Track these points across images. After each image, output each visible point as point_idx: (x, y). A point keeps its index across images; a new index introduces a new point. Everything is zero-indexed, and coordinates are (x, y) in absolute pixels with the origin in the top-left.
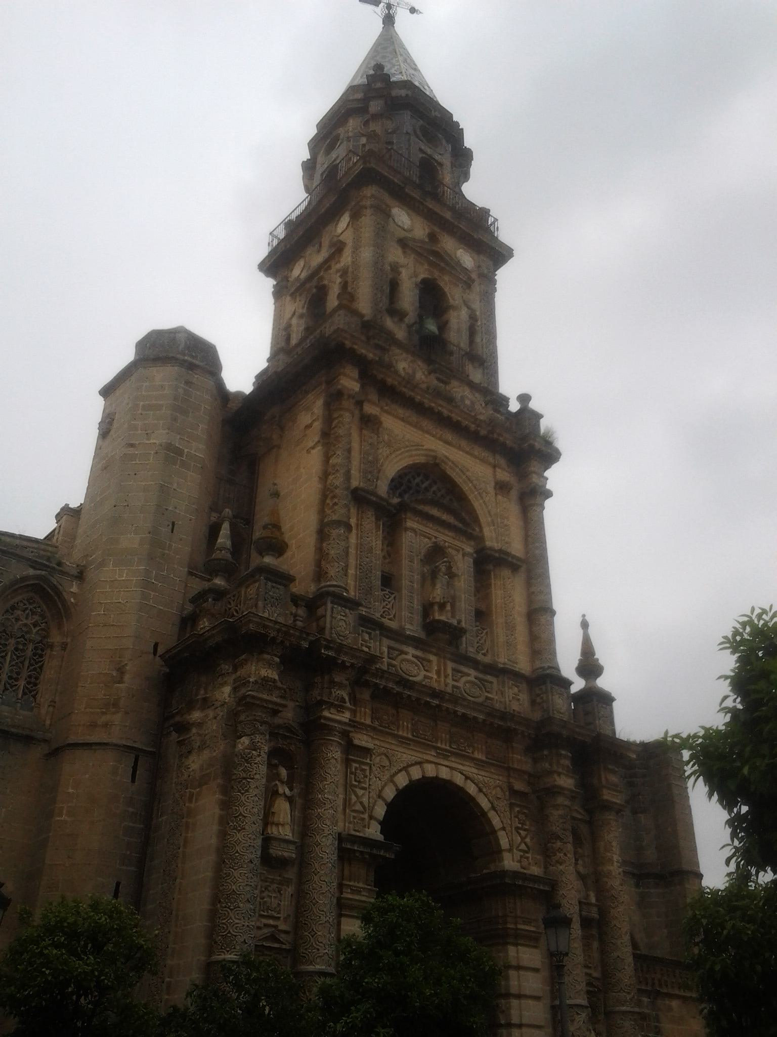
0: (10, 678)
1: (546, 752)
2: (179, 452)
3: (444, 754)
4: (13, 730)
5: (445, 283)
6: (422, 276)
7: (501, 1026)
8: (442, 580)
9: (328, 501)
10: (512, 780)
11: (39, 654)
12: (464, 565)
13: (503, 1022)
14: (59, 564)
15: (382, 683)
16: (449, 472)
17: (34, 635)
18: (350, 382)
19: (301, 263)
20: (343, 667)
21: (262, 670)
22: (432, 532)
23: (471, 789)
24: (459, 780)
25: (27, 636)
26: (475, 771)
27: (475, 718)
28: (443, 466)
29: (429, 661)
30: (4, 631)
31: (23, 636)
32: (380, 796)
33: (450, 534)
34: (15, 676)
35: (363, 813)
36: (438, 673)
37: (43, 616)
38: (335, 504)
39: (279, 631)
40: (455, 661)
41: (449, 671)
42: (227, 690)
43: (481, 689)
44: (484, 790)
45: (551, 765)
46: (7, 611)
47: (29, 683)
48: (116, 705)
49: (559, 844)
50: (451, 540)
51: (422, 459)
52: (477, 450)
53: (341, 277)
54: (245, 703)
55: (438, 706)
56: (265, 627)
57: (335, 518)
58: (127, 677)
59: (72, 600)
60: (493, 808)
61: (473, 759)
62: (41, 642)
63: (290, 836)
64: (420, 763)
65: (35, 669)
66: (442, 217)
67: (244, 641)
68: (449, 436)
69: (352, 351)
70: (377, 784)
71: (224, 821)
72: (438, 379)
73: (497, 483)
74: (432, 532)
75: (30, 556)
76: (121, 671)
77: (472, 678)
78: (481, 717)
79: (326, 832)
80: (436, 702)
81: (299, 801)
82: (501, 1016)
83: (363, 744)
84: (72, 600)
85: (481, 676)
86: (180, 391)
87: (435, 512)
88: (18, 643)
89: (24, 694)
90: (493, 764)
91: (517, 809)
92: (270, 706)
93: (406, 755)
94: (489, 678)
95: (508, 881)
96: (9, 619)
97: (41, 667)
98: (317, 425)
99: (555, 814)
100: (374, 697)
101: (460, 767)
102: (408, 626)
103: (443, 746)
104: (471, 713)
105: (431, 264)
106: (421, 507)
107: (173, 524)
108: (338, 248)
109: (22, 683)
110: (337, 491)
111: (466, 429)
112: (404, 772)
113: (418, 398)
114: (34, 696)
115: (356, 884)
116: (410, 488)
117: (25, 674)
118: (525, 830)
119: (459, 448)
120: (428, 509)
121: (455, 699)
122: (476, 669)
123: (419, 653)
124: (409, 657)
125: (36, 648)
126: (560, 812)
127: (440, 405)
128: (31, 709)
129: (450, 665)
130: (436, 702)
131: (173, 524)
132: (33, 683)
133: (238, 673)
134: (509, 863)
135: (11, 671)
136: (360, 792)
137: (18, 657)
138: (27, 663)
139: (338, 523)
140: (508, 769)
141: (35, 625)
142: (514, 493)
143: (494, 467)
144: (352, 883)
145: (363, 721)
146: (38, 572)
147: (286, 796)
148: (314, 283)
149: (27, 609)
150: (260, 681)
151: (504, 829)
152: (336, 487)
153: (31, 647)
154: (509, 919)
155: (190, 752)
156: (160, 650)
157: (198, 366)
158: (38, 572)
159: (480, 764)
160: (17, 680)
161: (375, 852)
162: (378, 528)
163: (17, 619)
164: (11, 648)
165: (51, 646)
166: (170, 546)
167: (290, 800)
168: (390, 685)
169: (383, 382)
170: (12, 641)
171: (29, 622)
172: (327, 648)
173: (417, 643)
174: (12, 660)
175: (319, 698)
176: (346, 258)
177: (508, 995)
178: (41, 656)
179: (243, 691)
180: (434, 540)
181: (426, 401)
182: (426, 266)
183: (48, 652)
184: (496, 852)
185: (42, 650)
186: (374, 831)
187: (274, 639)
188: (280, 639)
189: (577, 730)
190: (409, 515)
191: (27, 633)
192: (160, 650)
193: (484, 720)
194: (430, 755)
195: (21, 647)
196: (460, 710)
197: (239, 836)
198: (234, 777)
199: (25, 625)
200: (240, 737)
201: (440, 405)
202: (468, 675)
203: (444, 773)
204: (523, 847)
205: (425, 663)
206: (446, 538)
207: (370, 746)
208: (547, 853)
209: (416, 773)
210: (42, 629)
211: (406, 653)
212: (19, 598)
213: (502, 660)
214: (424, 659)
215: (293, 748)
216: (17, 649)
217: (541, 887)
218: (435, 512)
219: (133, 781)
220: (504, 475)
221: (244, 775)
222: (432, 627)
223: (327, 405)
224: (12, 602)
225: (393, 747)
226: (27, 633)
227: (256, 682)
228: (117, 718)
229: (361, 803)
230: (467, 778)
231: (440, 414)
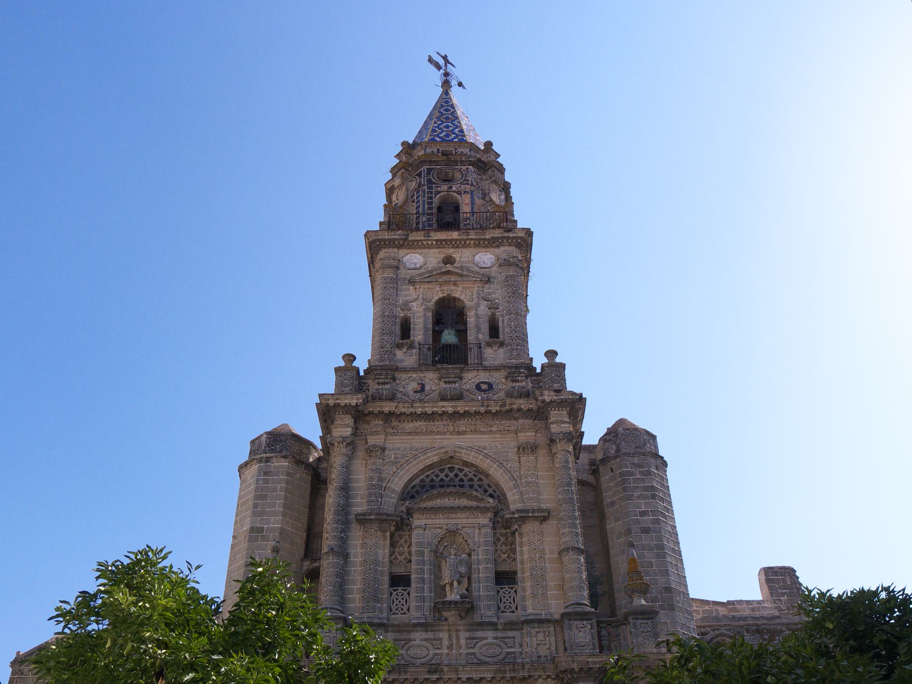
2: (260, 530)
22: (442, 521)
29: (440, 639)
33: (463, 516)
40: (469, 630)
41: (463, 642)
43: (499, 646)
50: (465, 521)
66: (451, 241)
69: (337, 406)
72: (445, 382)
74: (442, 521)
77: (490, 640)
80: (435, 677)
85: (500, 634)
86: (261, 482)
94: (510, 634)
119: (476, 432)
122: (497, 630)
123: (424, 635)
124: (417, 642)
127: (443, 407)
162: (385, 539)
169: (381, 413)
180: (445, 527)
181: (427, 409)
189: (590, 660)
190: (415, 516)
201: (443, 407)
206: (458, 521)
214: (435, 639)
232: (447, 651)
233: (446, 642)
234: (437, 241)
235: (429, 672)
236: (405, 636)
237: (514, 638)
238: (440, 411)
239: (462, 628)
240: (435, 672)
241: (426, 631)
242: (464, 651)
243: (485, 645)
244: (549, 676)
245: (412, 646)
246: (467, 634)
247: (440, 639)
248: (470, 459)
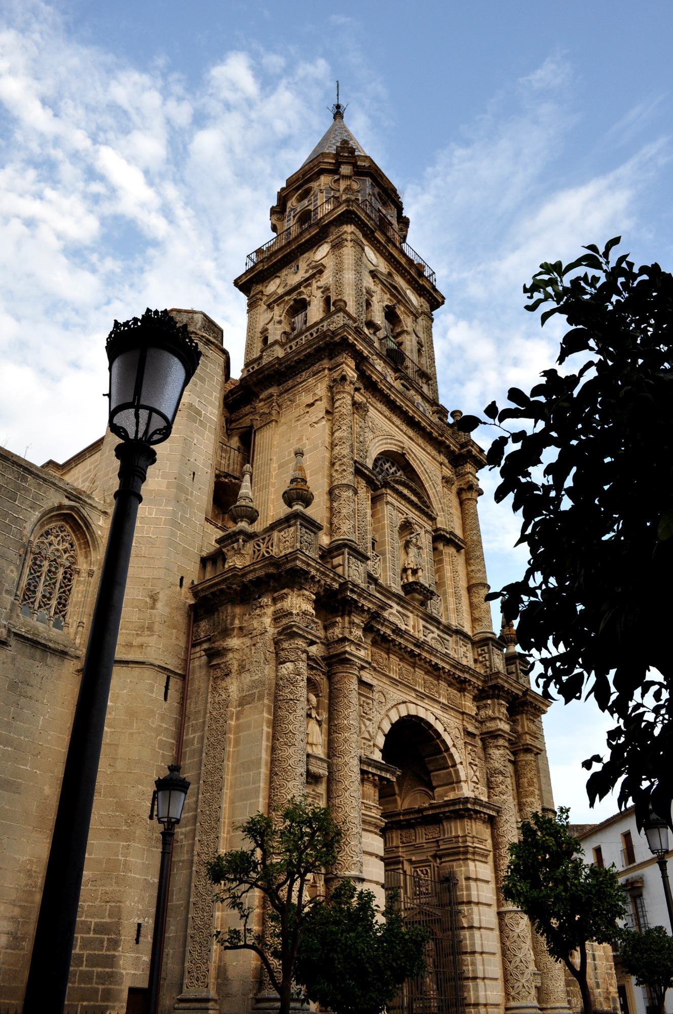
0: (44, 596)
1: (489, 702)
2: (199, 413)
3: (422, 696)
4: (50, 645)
5: (400, 310)
6: (386, 303)
7: (464, 928)
8: (413, 551)
9: (337, 467)
10: (465, 723)
11: (68, 578)
12: (425, 540)
13: (466, 925)
14: (89, 497)
15: (383, 630)
16: (412, 462)
17: (64, 560)
18: (349, 370)
19: (277, 281)
20: (362, 610)
21: (299, 603)
23: (439, 728)
24: (431, 720)
25: (59, 560)
26: (441, 713)
27: (443, 668)
28: (407, 456)
29: (408, 617)
30: (40, 553)
31: (55, 560)
32: (379, 728)
34: (48, 595)
35: (370, 741)
36: (414, 627)
37: (72, 545)
38: (344, 470)
42: (267, 621)
45: (493, 712)
46: (42, 536)
47: (59, 603)
48: (150, 628)
49: (501, 778)
51: (394, 448)
52: (429, 448)
53: (323, 292)
54: (288, 633)
55: (419, 655)
56: (308, 565)
57: (344, 482)
58: (159, 605)
59: (99, 533)
60: (454, 746)
62: (69, 567)
63: (322, 756)
64: (404, 702)
65: (64, 592)
67: (283, 576)
68: (411, 433)
69: (353, 346)
70: (377, 717)
71: (274, 737)
72: (403, 385)
73: (443, 478)
75: (67, 488)
76: (154, 599)
78: (447, 667)
79: (353, 754)
81: (325, 726)
82: (464, 920)
83: (369, 681)
84: (99, 533)
85: (441, 634)
87: (406, 491)
88: (50, 565)
89: (56, 613)
90: (452, 709)
91: (470, 747)
92: (310, 637)
93: (396, 694)
95: (469, 806)
96: (43, 543)
97: (69, 590)
98: (323, 405)
99: (496, 753)
102: (393, 585)
104: (441, 664)
105: (392, 295)
106: (397, 486)
107: (194, 474)
108: (319, 270)
109: (54, 602)
110: (345, 460)
111: (424, 429)
112: (395, 709)
113: (393, 397)
114: (64, 616)
116: (382, 471)
117: (56, 595)
120: (401, 488)
122: (438, 628)
124: (394, 611)
125: (65, 573)
126: (501, 752)
128: (61, 628)
129: (422, 622)
130: (417, 651)
131: (194, 474)
132: (63, 604)
133: (279, 606)
134: (467, 791)
135: (45, 590)
136: (368, 723)
137: (51, 579)
138: (58, 585)
139: (348, 486)
140: (463, 713)
141: (65, 552)
142: (454, 489)
143: (441, 464)
146: (72, 503)
147: (317, 720)
148: (294, 296)
149: (58, 535)
151: (461, 763)
152: (344, 457)
153: (61, 570)
154: (468, 839)
155: (227, 675)
156: (187, 583)
157: (212, 343)
158: (72, 503)
159: (445, 707)
160: (49, 599)
161: (383, 774)
163: (50, 544)
164: (45, 569)
165: (78, 573)
166: (192, 493)
167: (319, 723)
168: (389, 632)
170: (46, 563)
171: (60, 547)
172: (352, 591)
173: (400, 600)
174: (46, 580)
175: (340, 636)
176: (327, 278)
177: (469, 903)
178: (70, 580)
179: (285, 621)
182: (388, 296)
183: (75, 577)
184: (454, 782)
185: (71, 575)
186: (377, 756)
187: (313, 577)
191: (59, 557)
192: (187, 583)
194: (411, 697)
195: (53, 569)
196: (435, 660)
197: (291, 750)
198: (281, 698)
199: (58, 550)
200: (284, 662)
202: (433, 632)
203: (422, 714)
204: (475, 779)
207: (374, 682)
208: (490, 786)
210: (72, 556)
211: (391, 607)
212: (53, 525)
213: (454, 623)
214: (404, 615)
215: (318, 678)
216: (49, 571)
218: (406, 491)
219: (166, 699)
220: (448, 472)
221: (292, 697)
222: (409, 588)
223: (330, 388)
224: (46, 528)
226: (59, 557)
227: (298, 614)
228: (152, 641)
229: (368, 732)
230: (437, 718)
231: (406, 413)
234: (390, 254)
238: (405, 408)
248: (415, 466)
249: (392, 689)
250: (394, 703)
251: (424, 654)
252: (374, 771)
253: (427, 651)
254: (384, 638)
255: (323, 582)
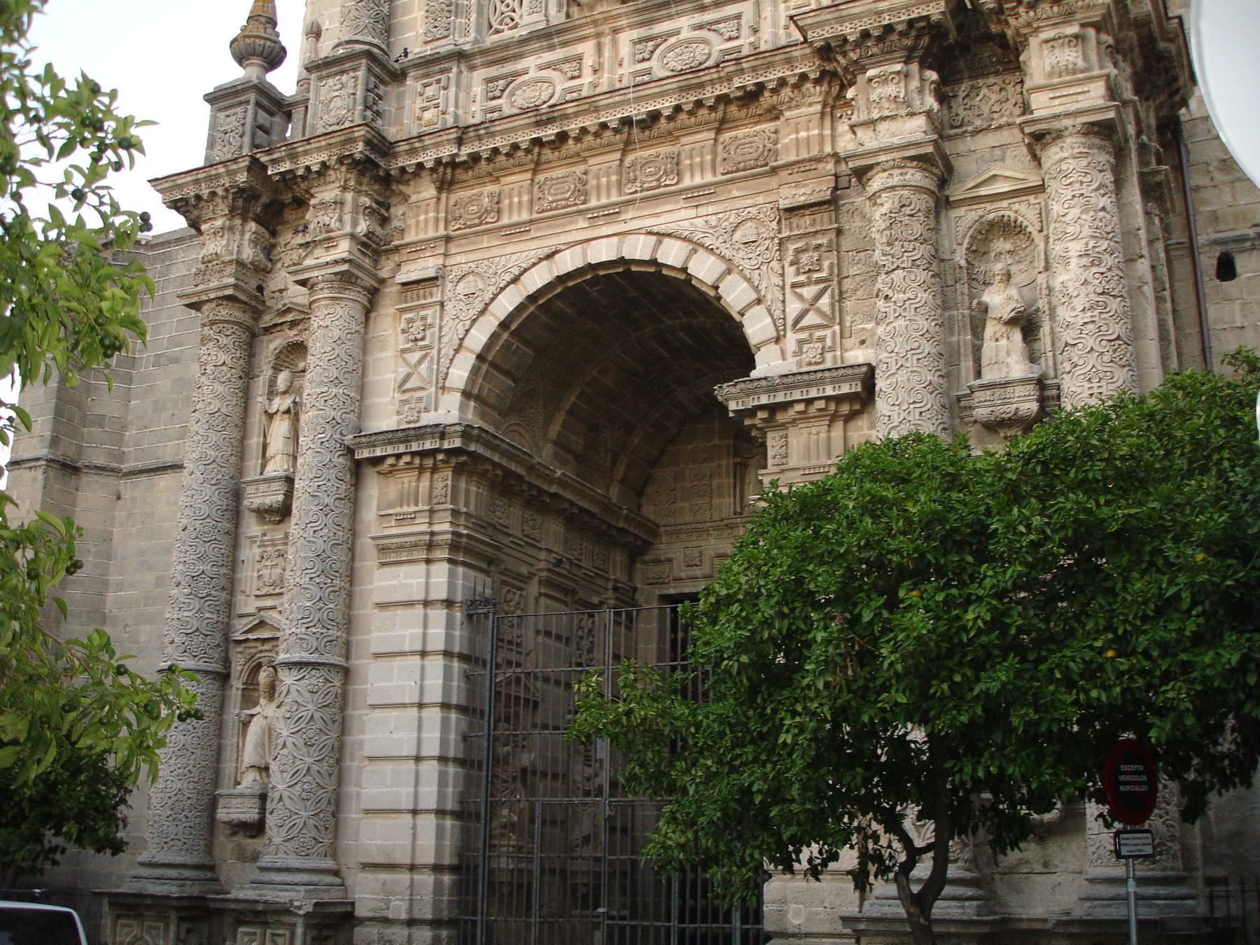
3: (611, 213)
23: (672, 254)
24: (638, 249)
26: (693, 213)
27: (655, 116)
39: (197, 182)
41: (625, 50)
44: (707, 242)
55: (562, 137)
61: (681, 192)
80: (550, 132)
92: (212, 296)
100: (445, 186)
101: (648, 222)
103: (604, 201)
115: (405, 509)
118: (818, 281)
121: (590, 104)
144: (398, 510)
145: (422, 236)
150: (203, 267)
168: (446, 152)
188: (205, 192)
193: (678, 109)
203: (602, 252)
205: (566, 67)
209: (537, 279)
217: (829, 391)
225: (494, 252)
232: (590, 79)
233: (588, 62)
235: (538, 124)
236: (509, 68)
237: (738, 17)
239: (624, 22)
240: (550, 121)
241: (551, 48)
242: (627, 69)
243: (672, 48)
244: (803, 77)
245: (519, 87)
246: (636, 34)
247: (579, 58)
249: (509, 249)
250: (508, 277)
251: (573, 126)
252: (390, 450)
253: (576, 114)
254: (453, 164)
255: (220, 192)
